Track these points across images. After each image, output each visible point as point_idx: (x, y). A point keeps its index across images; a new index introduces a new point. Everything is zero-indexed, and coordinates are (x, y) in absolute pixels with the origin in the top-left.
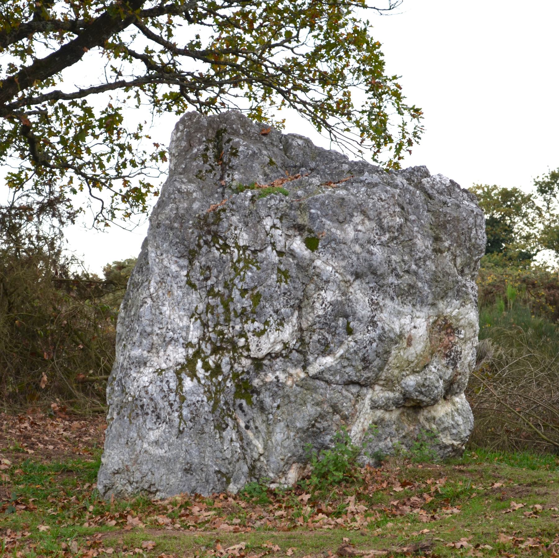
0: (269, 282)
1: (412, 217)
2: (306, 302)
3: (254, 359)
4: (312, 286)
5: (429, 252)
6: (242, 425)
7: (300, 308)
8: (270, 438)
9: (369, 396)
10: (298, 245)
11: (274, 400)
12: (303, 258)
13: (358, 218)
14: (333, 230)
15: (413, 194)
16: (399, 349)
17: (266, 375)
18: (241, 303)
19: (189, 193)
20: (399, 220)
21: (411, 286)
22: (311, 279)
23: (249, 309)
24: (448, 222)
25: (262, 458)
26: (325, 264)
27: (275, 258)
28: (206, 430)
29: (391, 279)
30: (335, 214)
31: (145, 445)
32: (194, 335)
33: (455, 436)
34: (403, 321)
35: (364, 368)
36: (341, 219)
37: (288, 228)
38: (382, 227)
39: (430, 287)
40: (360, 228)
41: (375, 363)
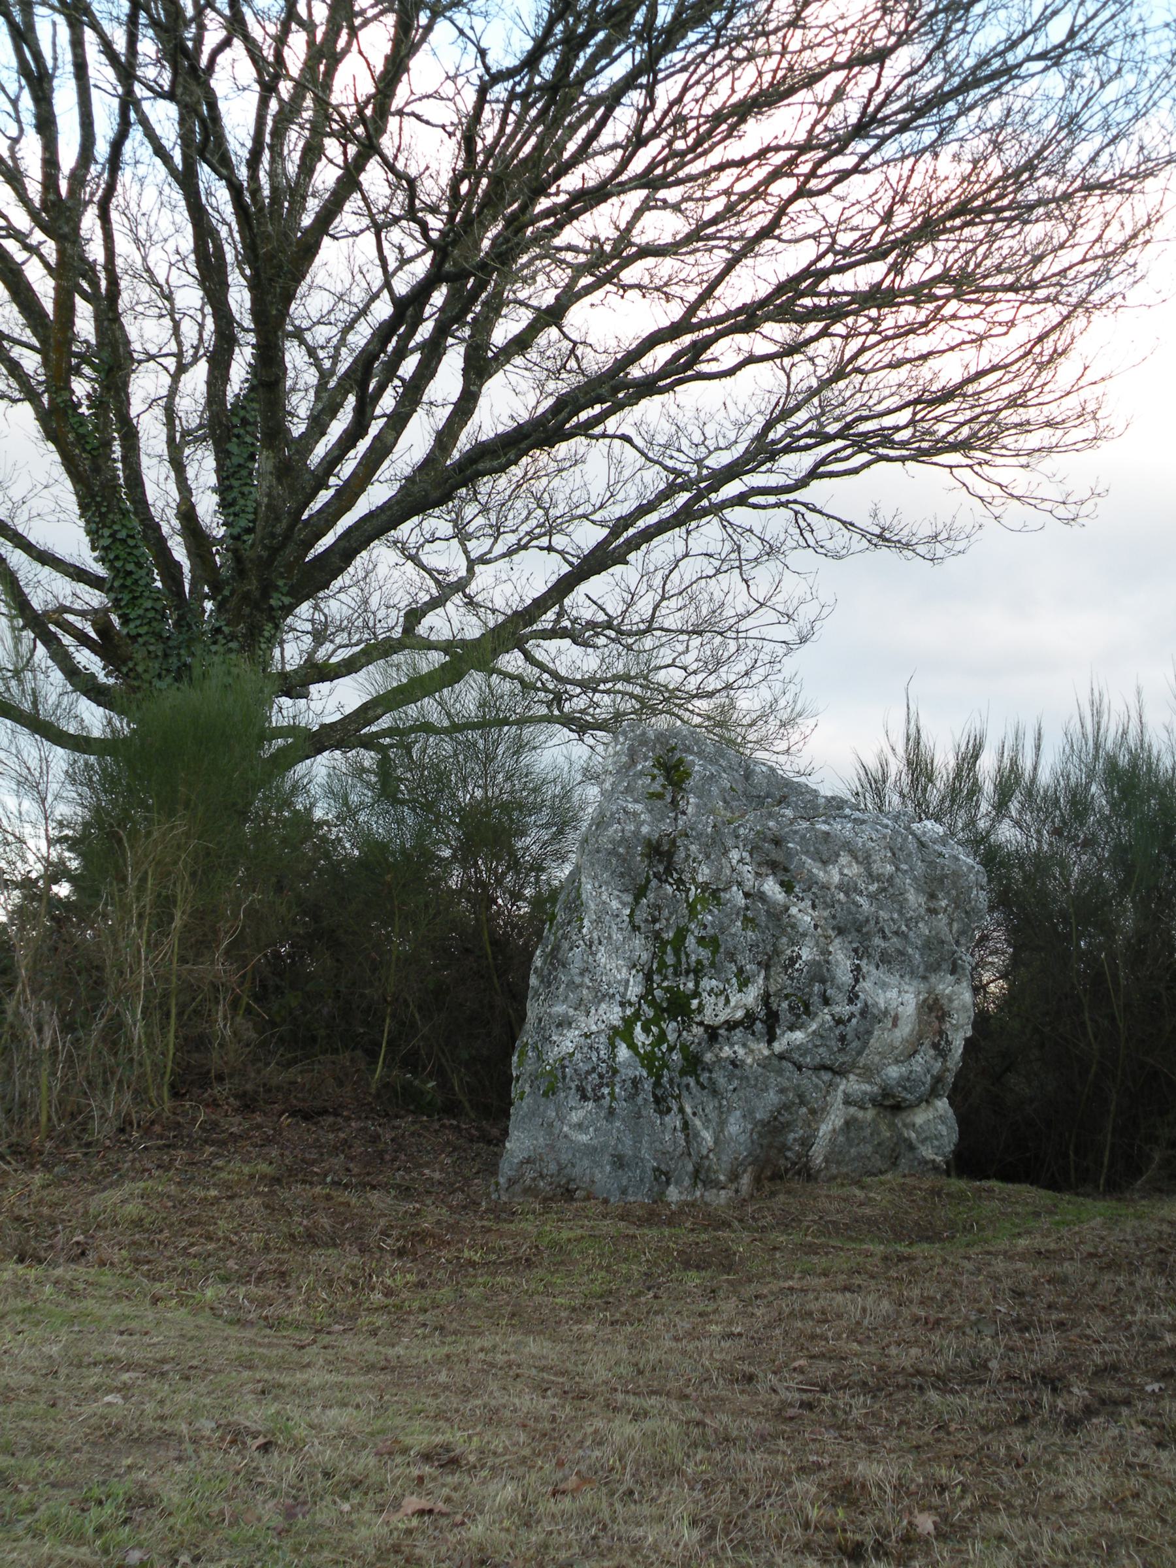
0: (733, 931)
1: (904, 867)
2: (776, 959)
3: (707, 1027)
4: (784, 940)
5: (922, 911)
6: (689, 1110)
7: (767, 967)
8: (722, 1131)
9: (842, 1087)
10: (771, 887)
11: (730, 1082)
12: (776, 903)
13: (844, 859)
14: (815, 871)
15: (905, 839)
16: (883, 1030)
17: (721, 1049)
18: (696, 952)
19: (635, 814)
20: (890, 869)
21: (901, 953)
22: (784, 930)
23: (706, 962)
24: (946, 876)
25: (711, 1155)
26: (803, 915)
27: (741, 901)
28: (644, 1113)
29: (877, 941)
30: (817, 851)
31: (565, 1129)
32: (634, 990)
33: (938, 1150)
34: (889, 995)
35: (840, 1050)
36: (824, 858)
37: (759, 865)
38: (870, 875)
39: (922, 955)
40: (846, 871)
41: (854, 1044)
